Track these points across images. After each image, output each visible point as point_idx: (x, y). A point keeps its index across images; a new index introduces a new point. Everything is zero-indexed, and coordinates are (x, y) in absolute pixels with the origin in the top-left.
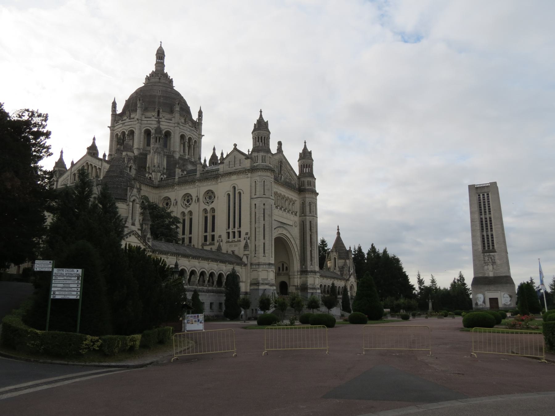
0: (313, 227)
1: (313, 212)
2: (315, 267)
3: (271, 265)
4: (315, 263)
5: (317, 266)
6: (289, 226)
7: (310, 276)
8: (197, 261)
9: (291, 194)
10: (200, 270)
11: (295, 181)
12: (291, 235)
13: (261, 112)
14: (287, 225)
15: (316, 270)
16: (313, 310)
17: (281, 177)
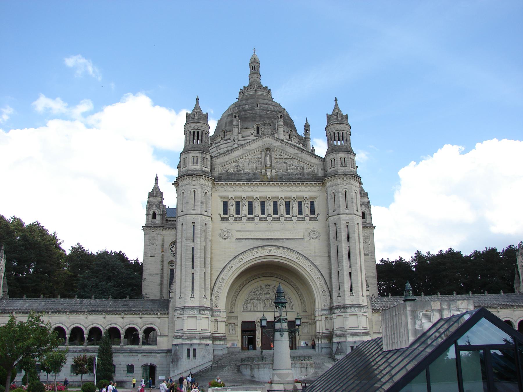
0: (339, 233)
1: (339, 207)
2: (344, 300)
3: (186, 310)
4: (344, 291)
5: (363, 296)
6: (290, 241)
7: (336, 315)
8: (65, 316)
9: (298, 189)
10: (71, 326)
11: (316, 167)
12: (299, 253)
13: (197, 99)
14: (285, 240)
15: (361, 303)
16: (82, 375)
17: (266, 171)
